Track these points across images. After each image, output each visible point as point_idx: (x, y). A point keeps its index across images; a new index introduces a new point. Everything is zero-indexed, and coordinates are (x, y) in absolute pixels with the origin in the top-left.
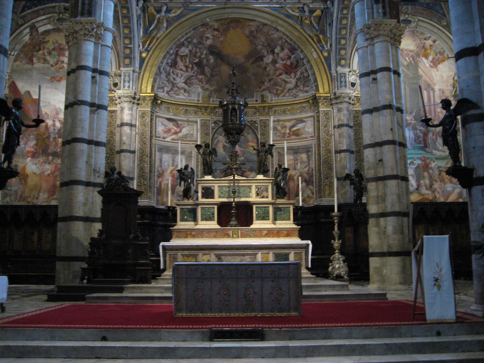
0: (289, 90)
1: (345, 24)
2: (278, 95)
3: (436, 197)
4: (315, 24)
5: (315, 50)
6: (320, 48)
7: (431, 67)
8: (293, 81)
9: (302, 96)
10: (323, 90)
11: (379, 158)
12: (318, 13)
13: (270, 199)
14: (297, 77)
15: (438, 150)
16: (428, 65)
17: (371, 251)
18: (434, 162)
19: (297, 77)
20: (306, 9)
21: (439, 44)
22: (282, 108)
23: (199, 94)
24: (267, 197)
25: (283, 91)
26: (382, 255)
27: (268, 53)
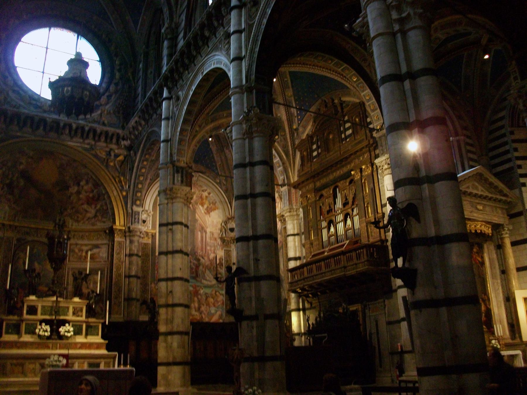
0: (89, 218)
1: (143, 173)
2: (78, 221)
3: (202, 317)
4: (118, 167)
5: (116, 189)
6: (120, 188)
7: (205, 213)
8: (93, 211)
9: (100, 225)
10: (119, 224)
11: (169, 289)
12: (121, 158)
13: (83, 318)
14: (97, 208)
15: (206, 280)
16: (203, 212)
17: (159, 361)
18: (202, 289)
19: (97, 208)
20: (113, 154)
21: (212, 196)
22: (81, 234)
23: (5, 213)
24: (82, 316)
25: (83, 219)
26: (168, 364)
27: (74, 185)
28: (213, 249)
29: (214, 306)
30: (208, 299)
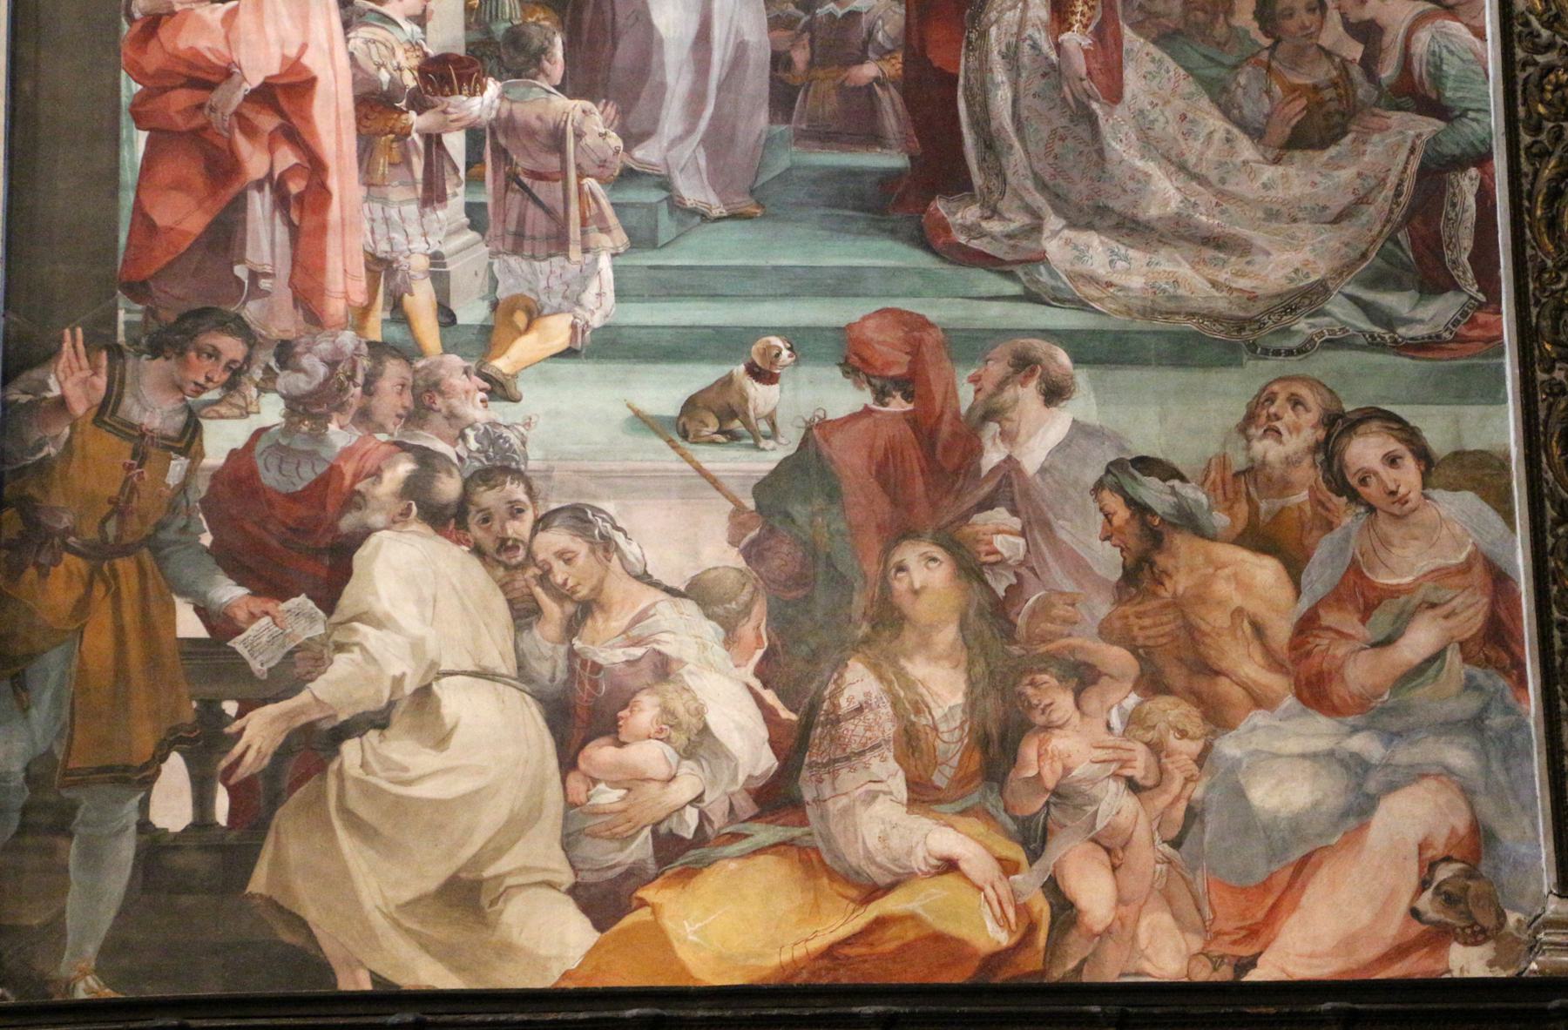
18: (1054, 393)
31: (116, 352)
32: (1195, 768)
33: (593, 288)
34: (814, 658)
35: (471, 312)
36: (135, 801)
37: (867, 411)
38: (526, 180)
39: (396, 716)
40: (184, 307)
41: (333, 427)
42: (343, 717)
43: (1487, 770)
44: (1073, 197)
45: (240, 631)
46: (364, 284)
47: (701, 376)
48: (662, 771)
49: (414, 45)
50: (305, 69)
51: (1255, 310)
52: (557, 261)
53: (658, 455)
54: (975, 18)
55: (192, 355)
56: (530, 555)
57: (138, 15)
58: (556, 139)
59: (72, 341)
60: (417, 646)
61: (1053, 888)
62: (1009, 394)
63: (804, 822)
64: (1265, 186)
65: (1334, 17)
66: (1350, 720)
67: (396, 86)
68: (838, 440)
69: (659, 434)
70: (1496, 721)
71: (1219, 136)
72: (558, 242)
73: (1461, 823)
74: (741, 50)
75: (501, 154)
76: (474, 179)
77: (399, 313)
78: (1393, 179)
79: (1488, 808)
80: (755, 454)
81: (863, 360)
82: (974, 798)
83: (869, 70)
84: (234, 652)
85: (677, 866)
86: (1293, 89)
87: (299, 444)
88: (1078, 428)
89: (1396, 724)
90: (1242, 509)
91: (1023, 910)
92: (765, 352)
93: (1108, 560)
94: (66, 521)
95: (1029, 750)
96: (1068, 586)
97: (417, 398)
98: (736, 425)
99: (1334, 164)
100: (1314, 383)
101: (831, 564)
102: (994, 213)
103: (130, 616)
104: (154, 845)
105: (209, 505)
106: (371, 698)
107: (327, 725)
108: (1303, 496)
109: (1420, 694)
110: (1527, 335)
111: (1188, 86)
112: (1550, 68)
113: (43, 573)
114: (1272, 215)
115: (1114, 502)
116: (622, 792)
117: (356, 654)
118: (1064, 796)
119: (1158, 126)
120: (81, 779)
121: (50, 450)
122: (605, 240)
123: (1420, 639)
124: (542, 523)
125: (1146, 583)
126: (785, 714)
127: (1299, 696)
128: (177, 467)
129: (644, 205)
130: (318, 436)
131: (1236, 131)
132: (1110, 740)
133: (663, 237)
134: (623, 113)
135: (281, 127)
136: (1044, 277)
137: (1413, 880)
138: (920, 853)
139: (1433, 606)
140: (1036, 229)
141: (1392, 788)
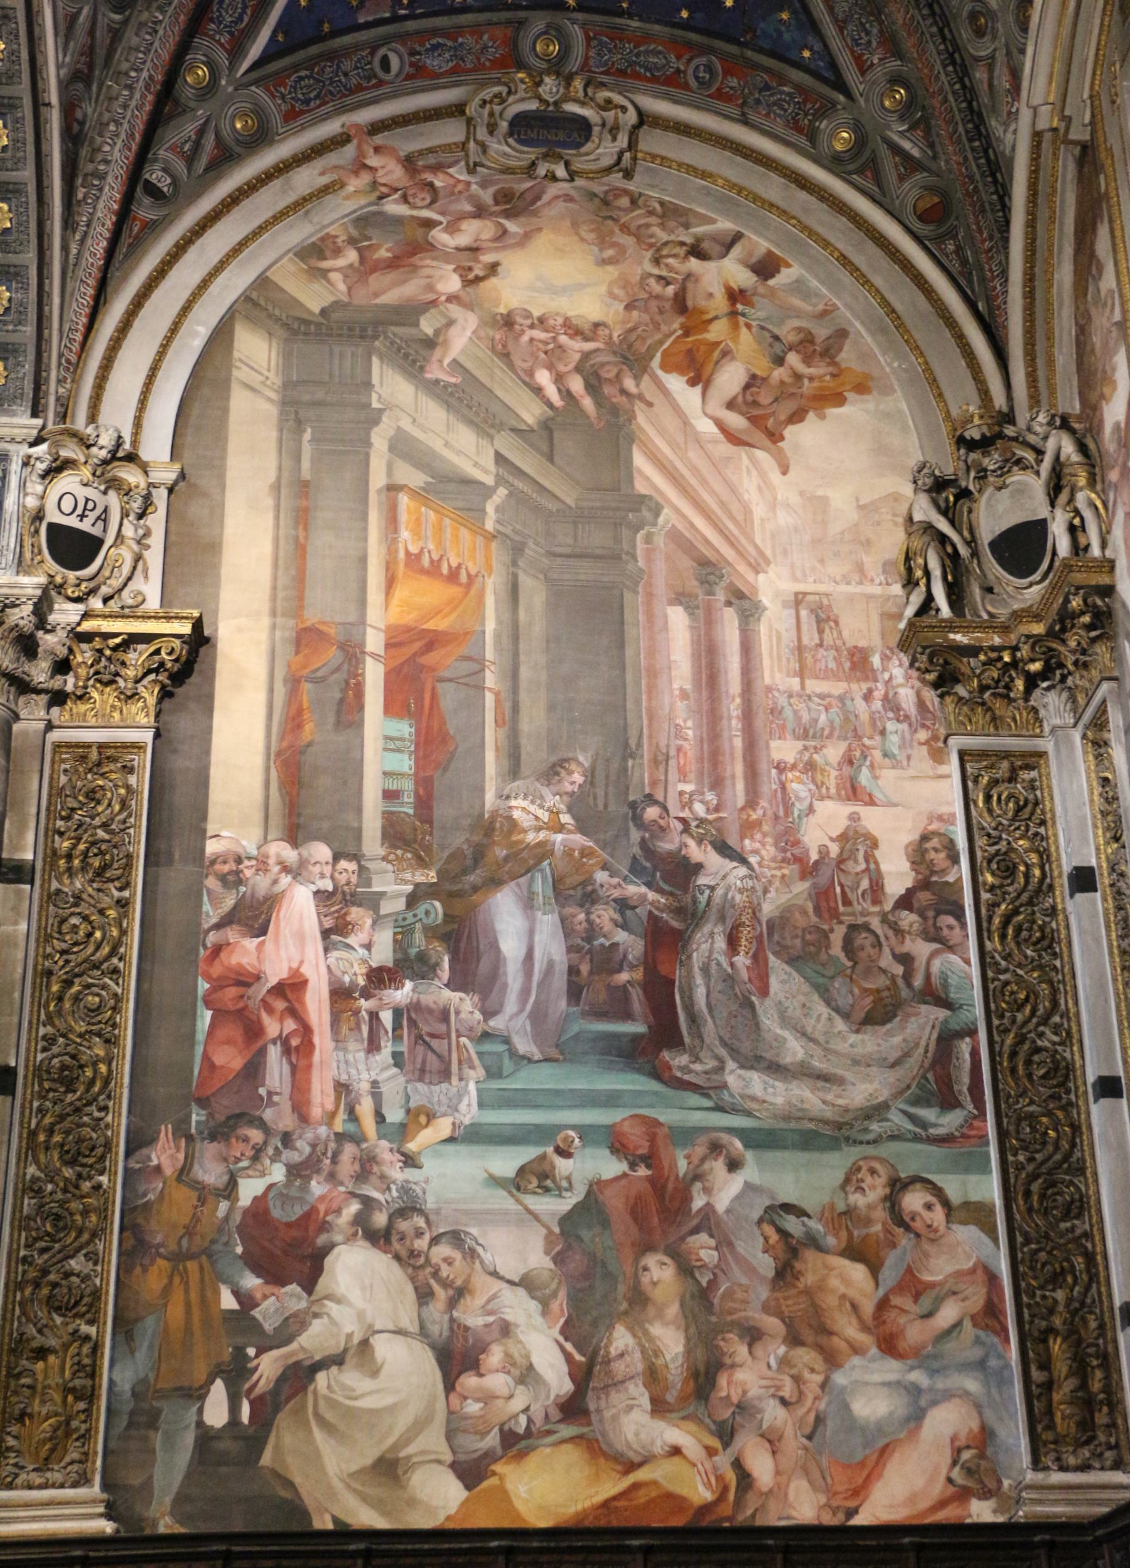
18: (734, 1165)
28: (833, 752)
29: (889, 1346)
30: (811, 1265)
31: (190, 1138)
32: (819, 1391)
33: (465, 1101)
34: (595, 1324)
35: (394, 1115)
36: (195, 1409)
37: (625, 1175)
38: (427, 1039)
39: (348, 1358)
40: (229, 1112)
41: (313, 1183)
42: (317, 1357)
43: (989, 1394)
44: (742, 1050)
45: (257, 1305)
46: (332, 1098)
47: (527, 1154)
48: (505, 1392)
49: (364, 961)
50: (302, 975)
51: (848, 1118)
52: (444, 1086)
53: (503, 1200)
54: (684, 947)
55: (233, 1140)
56: (428, 1260)
57: (209, 945)
58: (444, 1015)
59: (165, 1132)
60: (361, 1316)
61: (738, 1465)
62: (707, 1166)
63: (589, 1424)
64: (852, 1046)
65: (886, 951)
66: (909, 1362)
67: (353, 984)
68: (608, 1192)
69: (504, 1188)
70: (993, 1363)
71: (825, 1016)
72: (445, 1075)
73: (975, 1425)
74: (550, 966)
75: (413, 1023)
76: (397, 1038)
77: (353, 1115)
78: (923, 1043)
79: (990, 1416)
80: (560, 1200)
81: (623, 1145)
82: (691, 1409)
83: (624, 977)
84: (254, 1319)
85: (514, 1450)
86: (866, 991)
87: (293, 1192)
88: (748, 1186)
89: (936, 1365)
90: (844, 1234)
91: (720, 1478)
92: (565, 1139)
93: (766, 1265)
94: (159, 1239)
95: (722, 1380)
96: (744, 1280)
97: (362, 1167)
98: (549, 1183)
99: (890, 1034)
100: (882, 1160)
101: (604, 1265)
102: (697, 1059)
103: (194, 1296)
104: (206, 1437)
105: (241, 1229)
106: (333, 1346)
107: (307, 1363)
108: (877, 1228)
109: (950, 1346)
110: (1002, 1135)
111: (806, 988)
112: (1007, 983)
113: (145, 1270)
114: (856, 1062)
115: (769, 1230)
116: (481, 1405)
117: (325, 1319)
118: (743, 1408)
119: (790, 1010)
120: (162, 1395)
121: (151, 1196)
122: (472, 1073)
123: (948, 1314)
124: (435, 1241)
125: (789, 1278)
126: (578, 1357)
127: (879, 1347)
128: (223, 1206)
129: (493, 1053)
130: (305, 1188)
131: (833, 1014)
132: (770, 1374)
133: (505, 1073)
134: (484, 999)
135: (287, 1009)
136: (726, 1096)
137: (948, 1461)
138: (659, 1443)
139: (954, 1293)
140: (721, 1069)
141: (934, 1403)
